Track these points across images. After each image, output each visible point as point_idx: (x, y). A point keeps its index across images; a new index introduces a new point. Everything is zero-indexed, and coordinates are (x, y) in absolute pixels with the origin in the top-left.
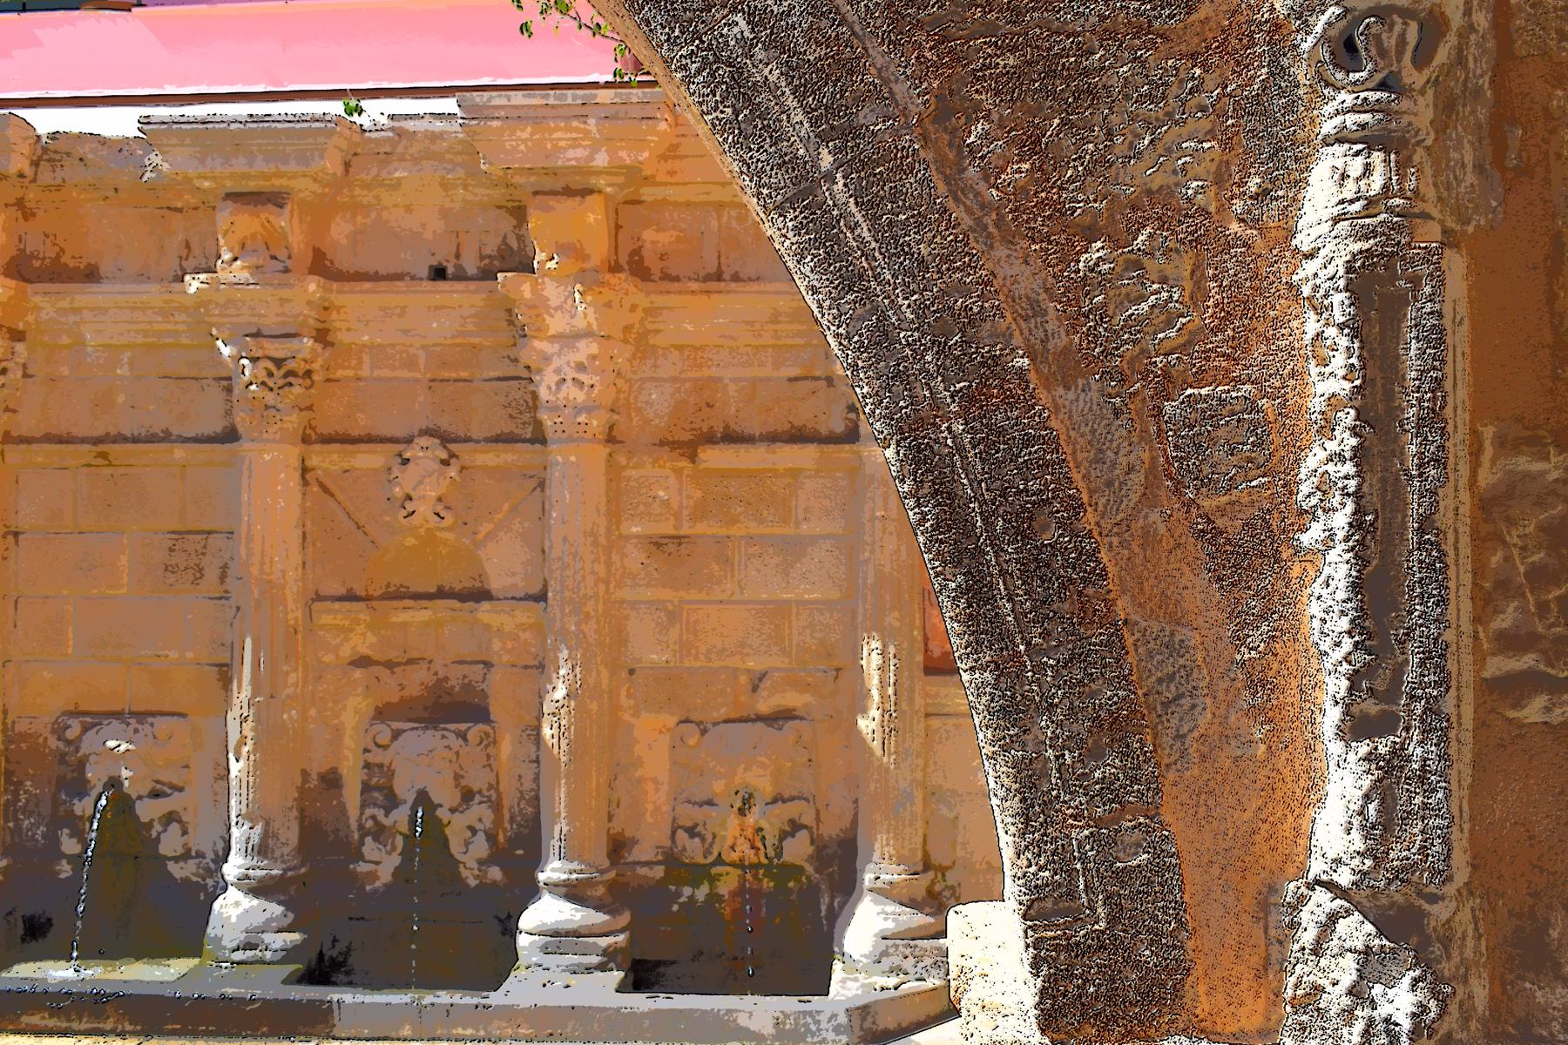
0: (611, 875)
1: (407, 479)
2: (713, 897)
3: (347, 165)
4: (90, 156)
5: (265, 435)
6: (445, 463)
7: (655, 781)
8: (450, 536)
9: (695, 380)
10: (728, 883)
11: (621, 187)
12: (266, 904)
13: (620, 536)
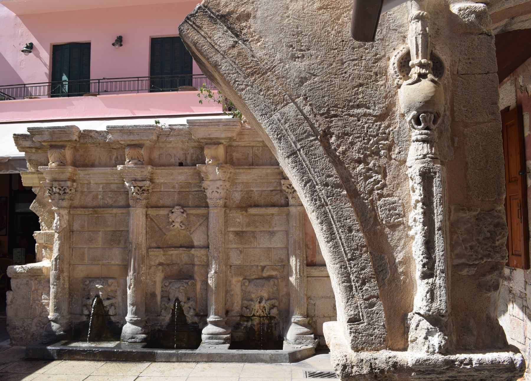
0: (226, 319)
1: (172, 217)
2: (252, 325)
3: (158, 137)
4: (93, 135)
6: (183, 213)
7: (237, 295)
8: (184, 231)
9: (247, 191)
10: (256, 321)
11: (229, 142)
12: (137, 327)
13: (228, 231)
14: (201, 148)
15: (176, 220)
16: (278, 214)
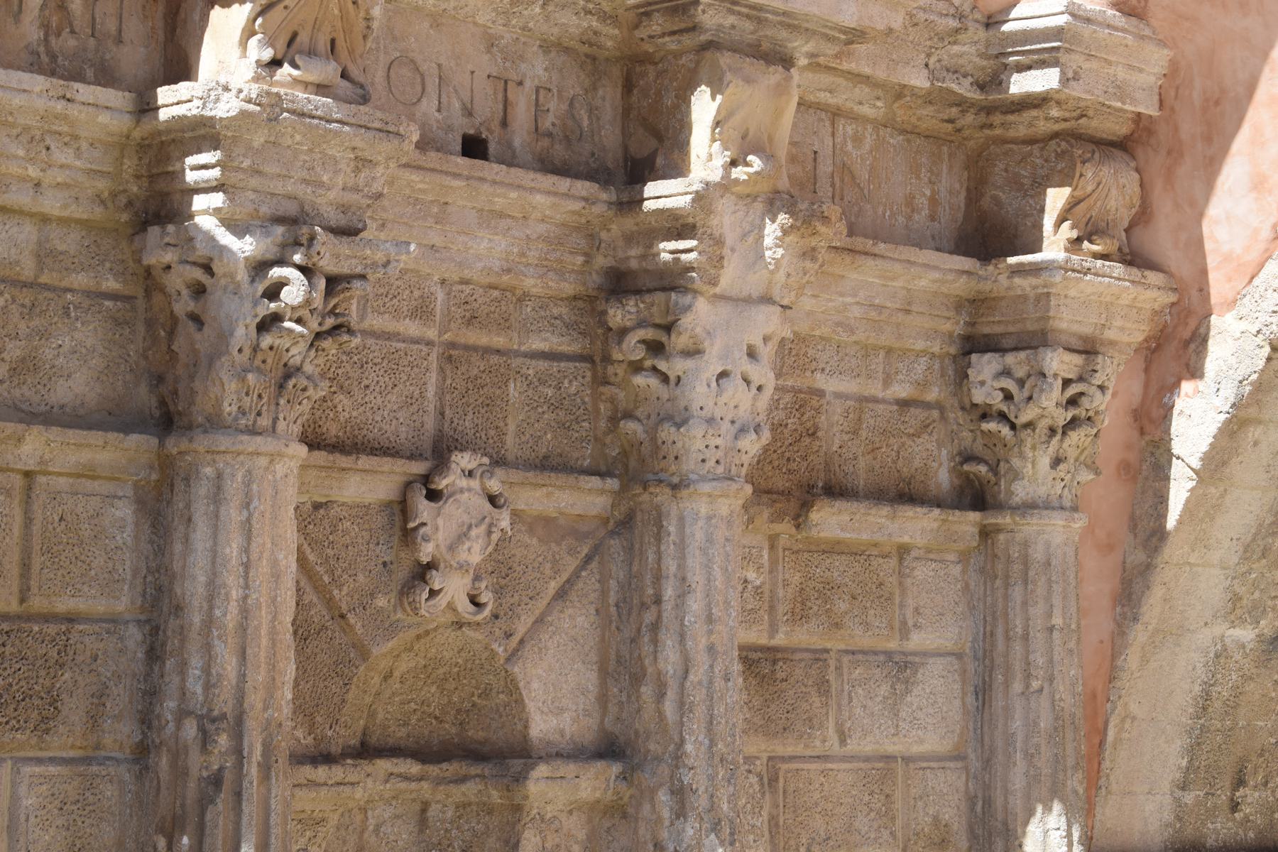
5: (281, 425)
14: (594, 59)
15: (463, 555)
16: (929, 551)
